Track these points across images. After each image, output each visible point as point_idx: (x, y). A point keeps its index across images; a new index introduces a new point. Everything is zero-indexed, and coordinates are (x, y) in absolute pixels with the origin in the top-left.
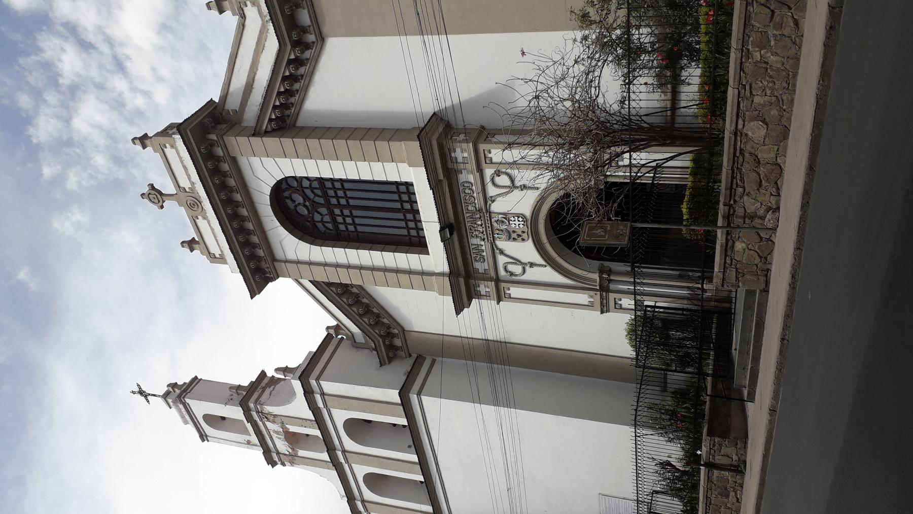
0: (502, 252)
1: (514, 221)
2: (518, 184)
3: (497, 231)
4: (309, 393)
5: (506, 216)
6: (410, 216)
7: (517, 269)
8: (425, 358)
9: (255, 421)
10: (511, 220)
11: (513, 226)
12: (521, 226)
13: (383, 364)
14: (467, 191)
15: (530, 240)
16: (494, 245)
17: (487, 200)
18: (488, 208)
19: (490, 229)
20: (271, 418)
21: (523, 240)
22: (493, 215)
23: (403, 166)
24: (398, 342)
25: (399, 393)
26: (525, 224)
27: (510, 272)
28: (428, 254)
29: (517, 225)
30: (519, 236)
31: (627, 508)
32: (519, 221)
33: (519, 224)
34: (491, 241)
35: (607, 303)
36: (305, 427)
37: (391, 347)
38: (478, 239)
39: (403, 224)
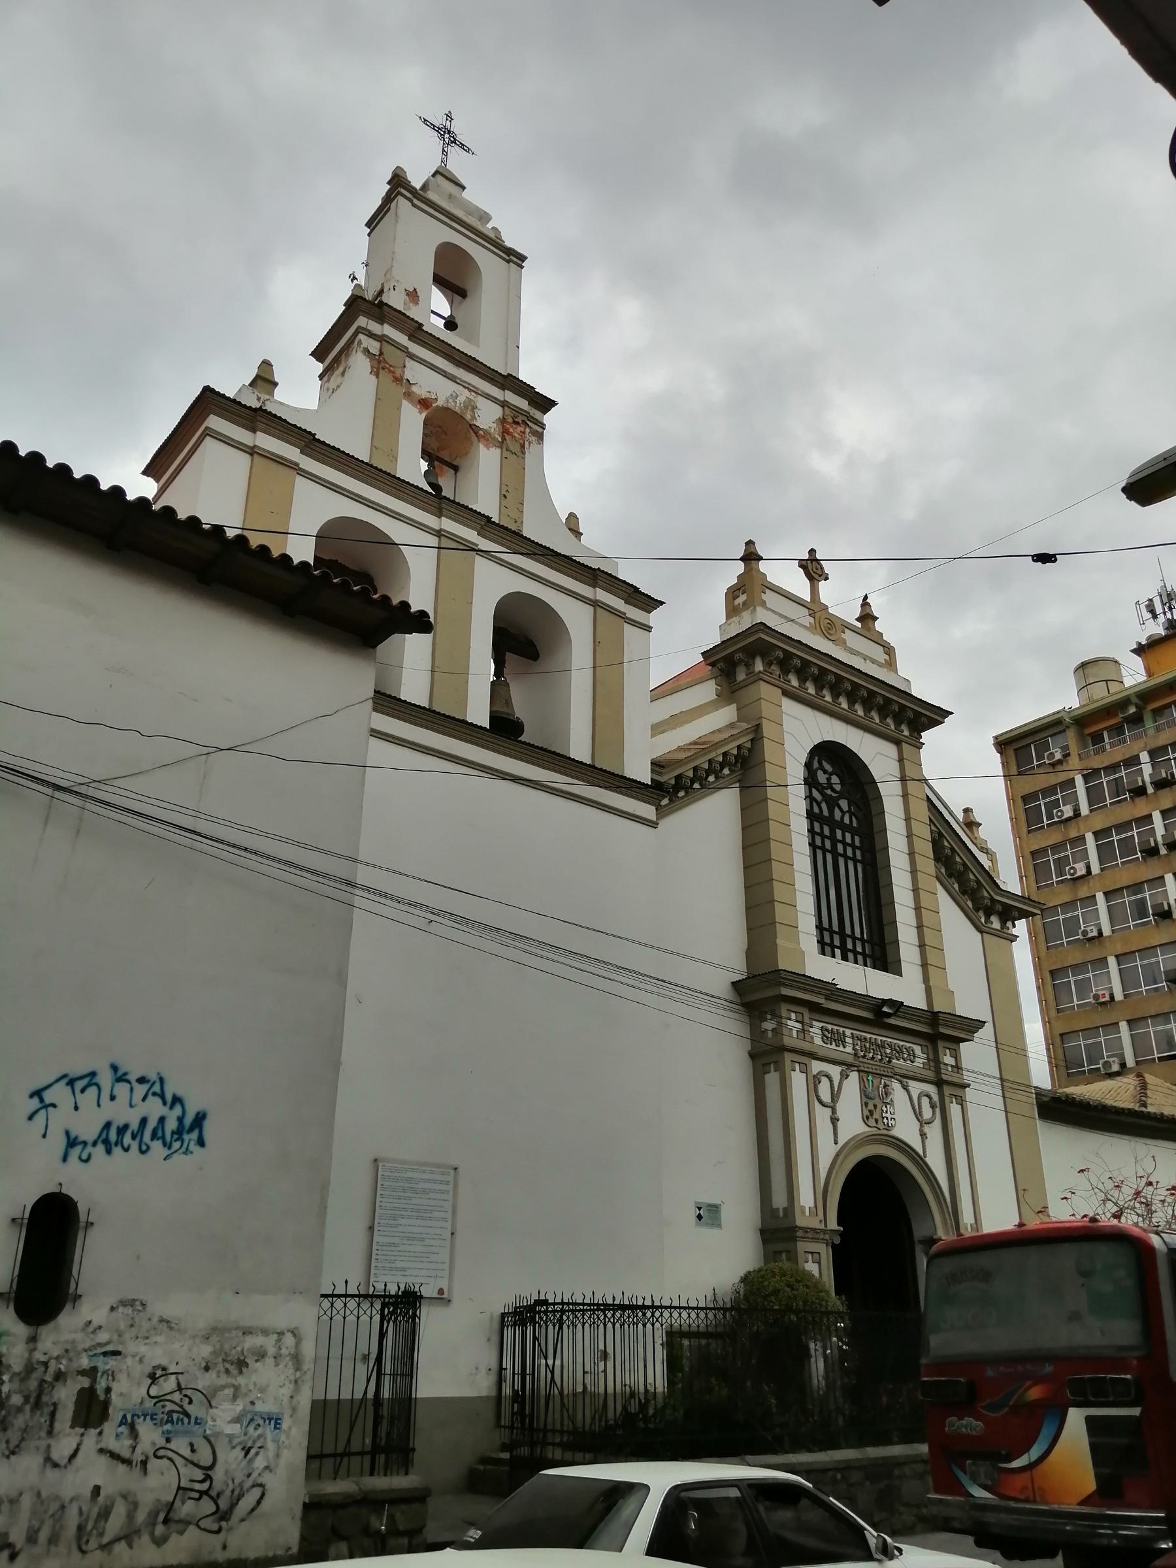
0: (846, 1078)
2: (926, 1129)
4: (629, 595)
9: (503, 387)
17: (904, 1078)
18: (896, 1077)
19: (874, 1071)
20: (516, 431)
21: (866, 1119)
22: (890, 1079)
30: (871, 1112)
31: (423, 1240)
32: (891, 1118)
33: (887, 1118)
35: (812, 1239)
36: (505, 496)
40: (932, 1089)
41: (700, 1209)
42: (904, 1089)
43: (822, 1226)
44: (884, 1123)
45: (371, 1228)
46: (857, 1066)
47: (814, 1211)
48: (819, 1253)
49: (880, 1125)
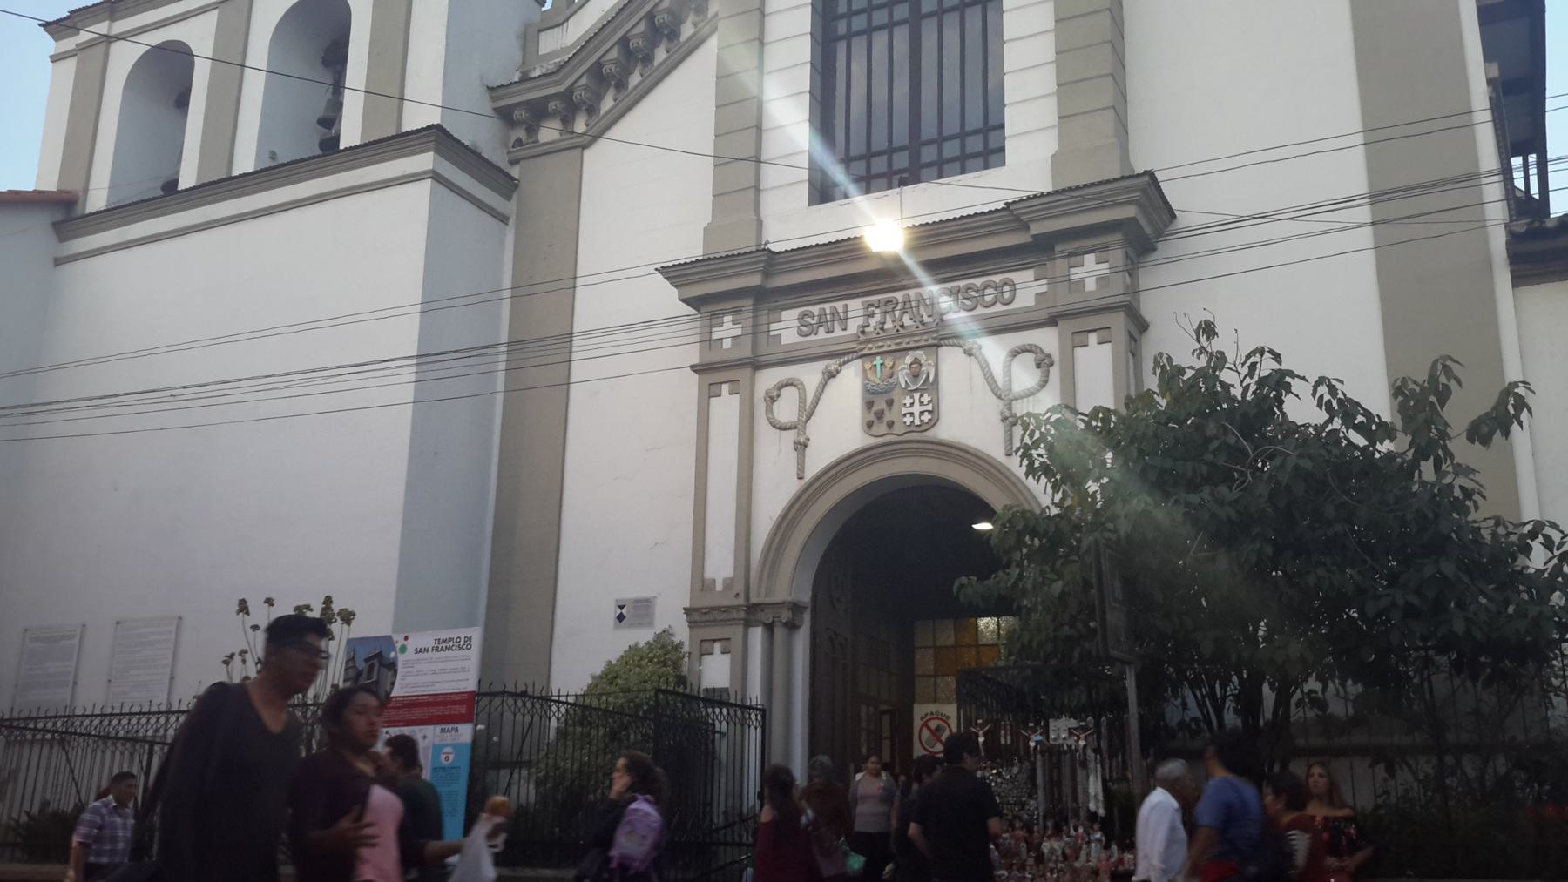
0: (834, 376)
1: (921, 403)
3: (891, 364)
5: (932, 384)
6: (901, 160)
7: (786, 410)
8: (508, 198)
10: (921, 396)
11: (908, 401)
12: (908, 420)
13: (494, 94)
14: (990, 295)
15: (872, 441)
16: (850, 356)
18: (946, 341)
21: (870, 425)
23: (1048, 144)
24: (549, 132)
25: (437, 128)
26: (915, 429)
27: (778, 396)
28: (812, 203)
29: (912, 408)
30: (880, 415)
32: (922, 413)
33: (912, 414)
34: (861, 350)
37: (538, 112)
38: (861, 321)
39: (879, 142)
40: (1048, 339)
41: (621, 607)
42: (970, 355)
43: (741, 601)
44: (905, 423)
45: (110, 681)
46: (856, 352)
47: (728, 584)
48: (729, 639)
49: (898, 429)
